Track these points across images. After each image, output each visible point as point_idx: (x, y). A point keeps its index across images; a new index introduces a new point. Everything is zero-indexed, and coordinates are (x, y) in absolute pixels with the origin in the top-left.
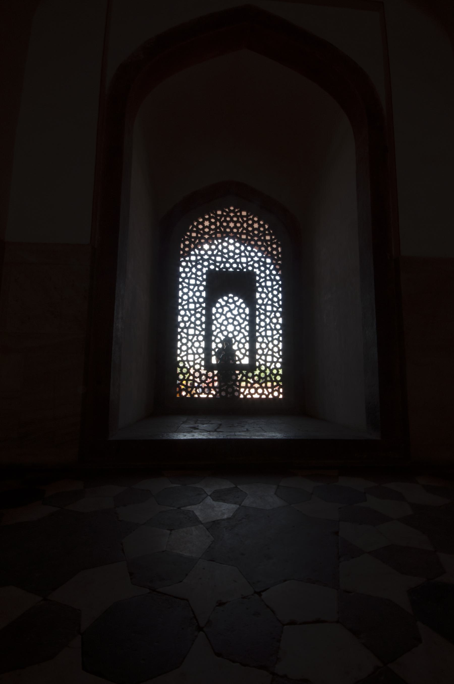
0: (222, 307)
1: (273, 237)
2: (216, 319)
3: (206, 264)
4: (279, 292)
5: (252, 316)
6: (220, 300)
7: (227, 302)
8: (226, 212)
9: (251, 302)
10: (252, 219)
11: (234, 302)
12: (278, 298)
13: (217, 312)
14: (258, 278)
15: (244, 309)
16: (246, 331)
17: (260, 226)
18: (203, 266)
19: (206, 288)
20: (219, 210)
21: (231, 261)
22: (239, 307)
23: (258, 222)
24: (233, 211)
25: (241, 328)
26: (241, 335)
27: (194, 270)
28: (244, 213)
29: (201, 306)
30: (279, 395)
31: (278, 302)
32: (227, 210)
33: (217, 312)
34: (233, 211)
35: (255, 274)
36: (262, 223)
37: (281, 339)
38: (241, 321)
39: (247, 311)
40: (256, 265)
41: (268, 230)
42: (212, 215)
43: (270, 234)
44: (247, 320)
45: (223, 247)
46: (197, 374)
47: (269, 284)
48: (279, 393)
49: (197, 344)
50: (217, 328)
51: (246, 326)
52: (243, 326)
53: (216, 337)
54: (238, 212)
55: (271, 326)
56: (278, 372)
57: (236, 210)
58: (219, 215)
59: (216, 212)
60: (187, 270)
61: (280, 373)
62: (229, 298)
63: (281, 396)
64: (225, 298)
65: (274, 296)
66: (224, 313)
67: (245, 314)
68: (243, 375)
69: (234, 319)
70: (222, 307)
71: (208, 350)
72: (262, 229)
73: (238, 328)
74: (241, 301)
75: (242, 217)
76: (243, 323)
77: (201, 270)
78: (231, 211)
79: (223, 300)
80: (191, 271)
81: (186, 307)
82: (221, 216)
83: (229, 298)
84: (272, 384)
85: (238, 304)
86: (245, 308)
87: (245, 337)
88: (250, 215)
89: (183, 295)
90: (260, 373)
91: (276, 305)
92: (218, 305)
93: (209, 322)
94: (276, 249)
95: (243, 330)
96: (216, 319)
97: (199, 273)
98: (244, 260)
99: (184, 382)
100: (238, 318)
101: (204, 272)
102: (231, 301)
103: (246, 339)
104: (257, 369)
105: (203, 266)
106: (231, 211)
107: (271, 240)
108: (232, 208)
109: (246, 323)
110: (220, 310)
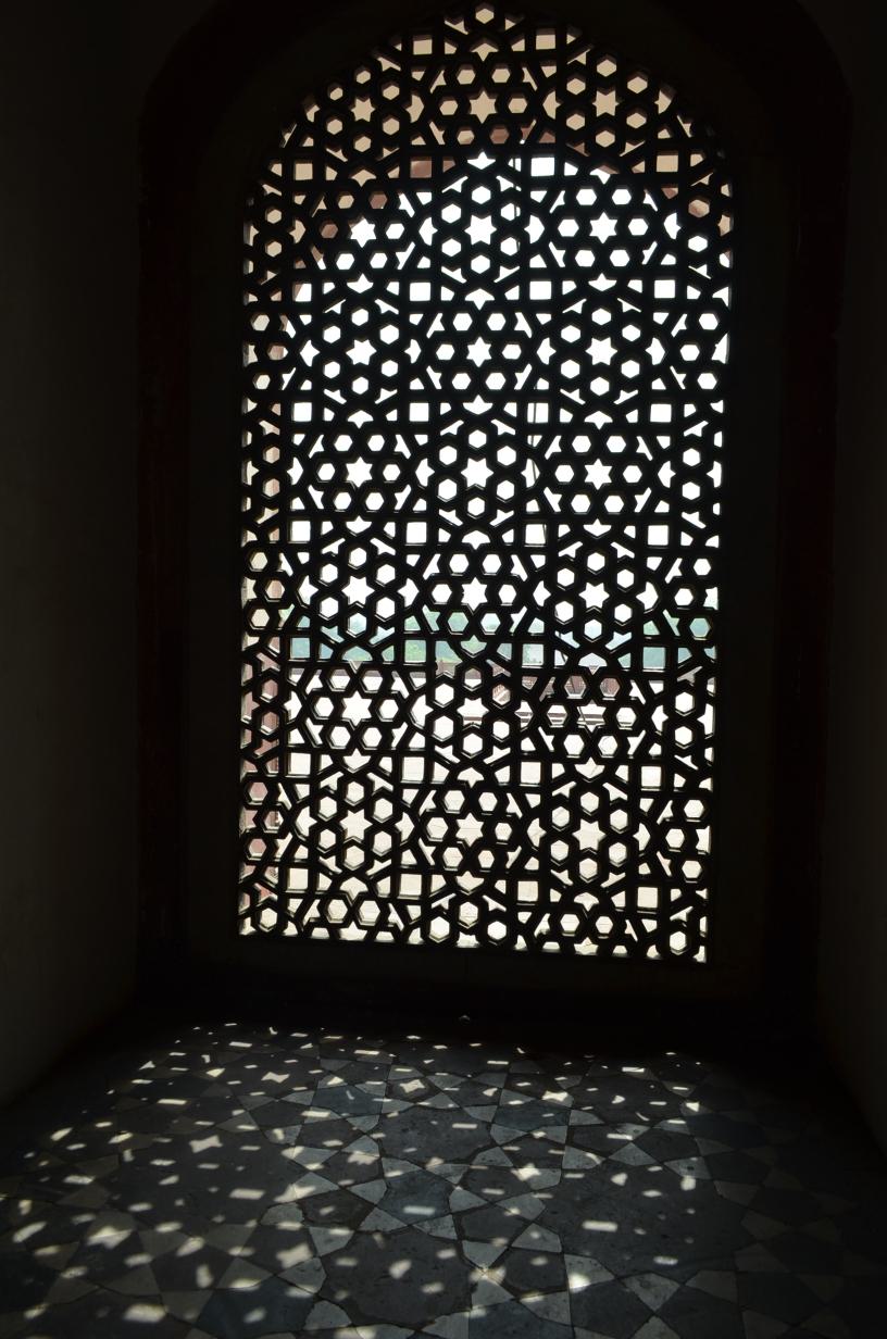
1: (696, 159)
4: (709, 454)
8: (455, 37)
12: (706, 483)
17: (628, 103)
20: (422, 35)
23: (617, 83)
24: (492, 32)
28: (546, 42)
32: (460, 27)
34: (492, 32)
36: (637, 85)
41: (668, 119)
42: (386, 64)
43: (680, 146)
47: (661, 413)
56: (691, 839)
58: (421, 61)
59: (408, 47)
65: (684, 474)
75: (535, 59)
78: (479, 32)
82: (432, 63)
88: (576, 48)
91: (693, 518)
106: (479, 32)
108: (485, 16)
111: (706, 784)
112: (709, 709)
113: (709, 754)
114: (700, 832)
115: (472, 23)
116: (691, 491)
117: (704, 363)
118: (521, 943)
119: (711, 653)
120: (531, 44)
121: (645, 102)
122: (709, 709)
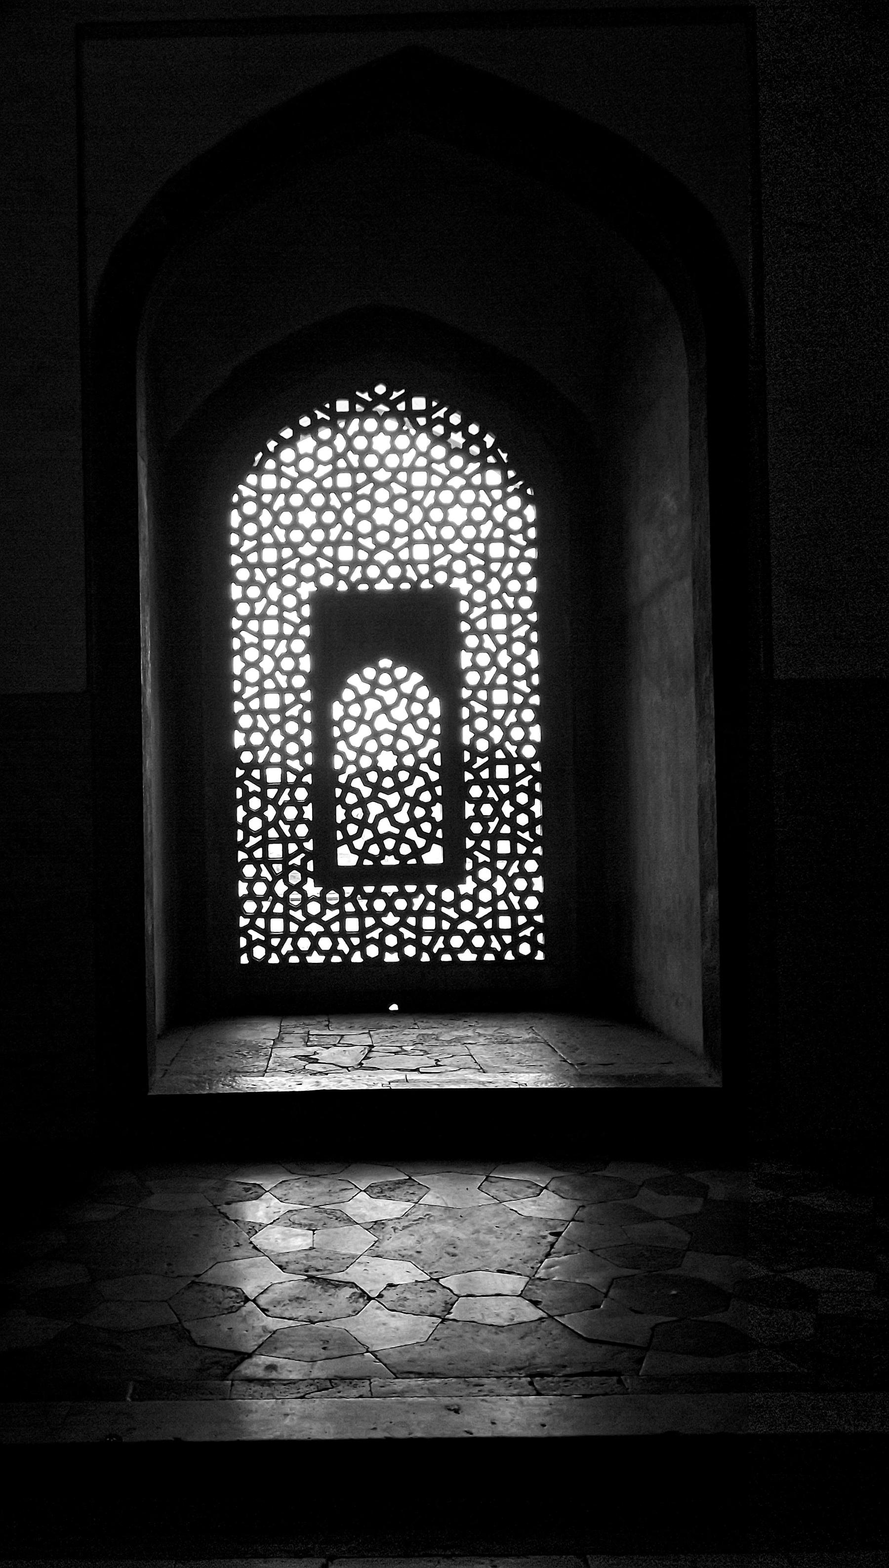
0: (360, 699)
1: (511, 474)
2: (345, 736)
3: (308, 570)
5: (451, 722)
6: (354, 680)
7: (374, 684)
8: (362, 402)
9: (445, 680)
10: (445, 421)
11: (396, 684)
13: (347, 716)
14: (464, 607)
15: (425, 703)
16: (433, 767)
17: (470, 440)
18: (301, 579)
19: (312, 646)
20: (343, 397)
21: (384, 557)
22: (412, 698)
23: (462, 428)
24: (383, 399)
26: (419, 782)
27: (274, 592)
28: (419, 403)
30: (533, 953)
31: (527, 677)
32: (366, 396)
34: (383, 399)
35: (454, 597)
38: (418, 739)
39: (435, 708)
40: (459, 567)
41: (493, 451)
42: (320, 415)
43: (500, 465)
45: (359, 517)
48: (535, 946)
49: (291, 813)
50: (347, 763)
51: (432, 753)
52: (423, 753)
54: (399, 400)
57: (395, 395)
58: (343, 415)
59: (333, 406)
60: (254, 592)
63: (540, 956)
64: (369, 672)
66: (368, 717)
68: (428, 898)
69: (397, 735)
70: (360, 699)
72: (475, 450)
73: (409, 760)
74: (417, 677)
76: (423, 745)
77: (292, 591)
78: (378, 399)
79: (364, 679)
83: (380, 671)
85: (407, 688)
86: (429, 699)
87: (429, 786)
89: (244, 670)
90: (476, 891)
91: (522, 685)
92: (348, 695)
94: (519, 513)
95: (424, 767)
96: (345, 736)
97: (290, 601)
98: (421, 552)
99: (260, 923)
101: (305, 596)
102: (385, 679)
103: (433, 793)
104: (469, 879)
105: (301, 579)
106: (378, 399)
108: (380, 389)
109: (433, 744)
110: (355, 710)
111: (538, 850)
112: (538, 802)
113: (539, 830)
114: (534, 880)
115: (372, 394)
117: (523, 592)
118: (425, 958)
119: (537, 767)
120: (409, 405)
121: (478, 440)
122: (538, 802)
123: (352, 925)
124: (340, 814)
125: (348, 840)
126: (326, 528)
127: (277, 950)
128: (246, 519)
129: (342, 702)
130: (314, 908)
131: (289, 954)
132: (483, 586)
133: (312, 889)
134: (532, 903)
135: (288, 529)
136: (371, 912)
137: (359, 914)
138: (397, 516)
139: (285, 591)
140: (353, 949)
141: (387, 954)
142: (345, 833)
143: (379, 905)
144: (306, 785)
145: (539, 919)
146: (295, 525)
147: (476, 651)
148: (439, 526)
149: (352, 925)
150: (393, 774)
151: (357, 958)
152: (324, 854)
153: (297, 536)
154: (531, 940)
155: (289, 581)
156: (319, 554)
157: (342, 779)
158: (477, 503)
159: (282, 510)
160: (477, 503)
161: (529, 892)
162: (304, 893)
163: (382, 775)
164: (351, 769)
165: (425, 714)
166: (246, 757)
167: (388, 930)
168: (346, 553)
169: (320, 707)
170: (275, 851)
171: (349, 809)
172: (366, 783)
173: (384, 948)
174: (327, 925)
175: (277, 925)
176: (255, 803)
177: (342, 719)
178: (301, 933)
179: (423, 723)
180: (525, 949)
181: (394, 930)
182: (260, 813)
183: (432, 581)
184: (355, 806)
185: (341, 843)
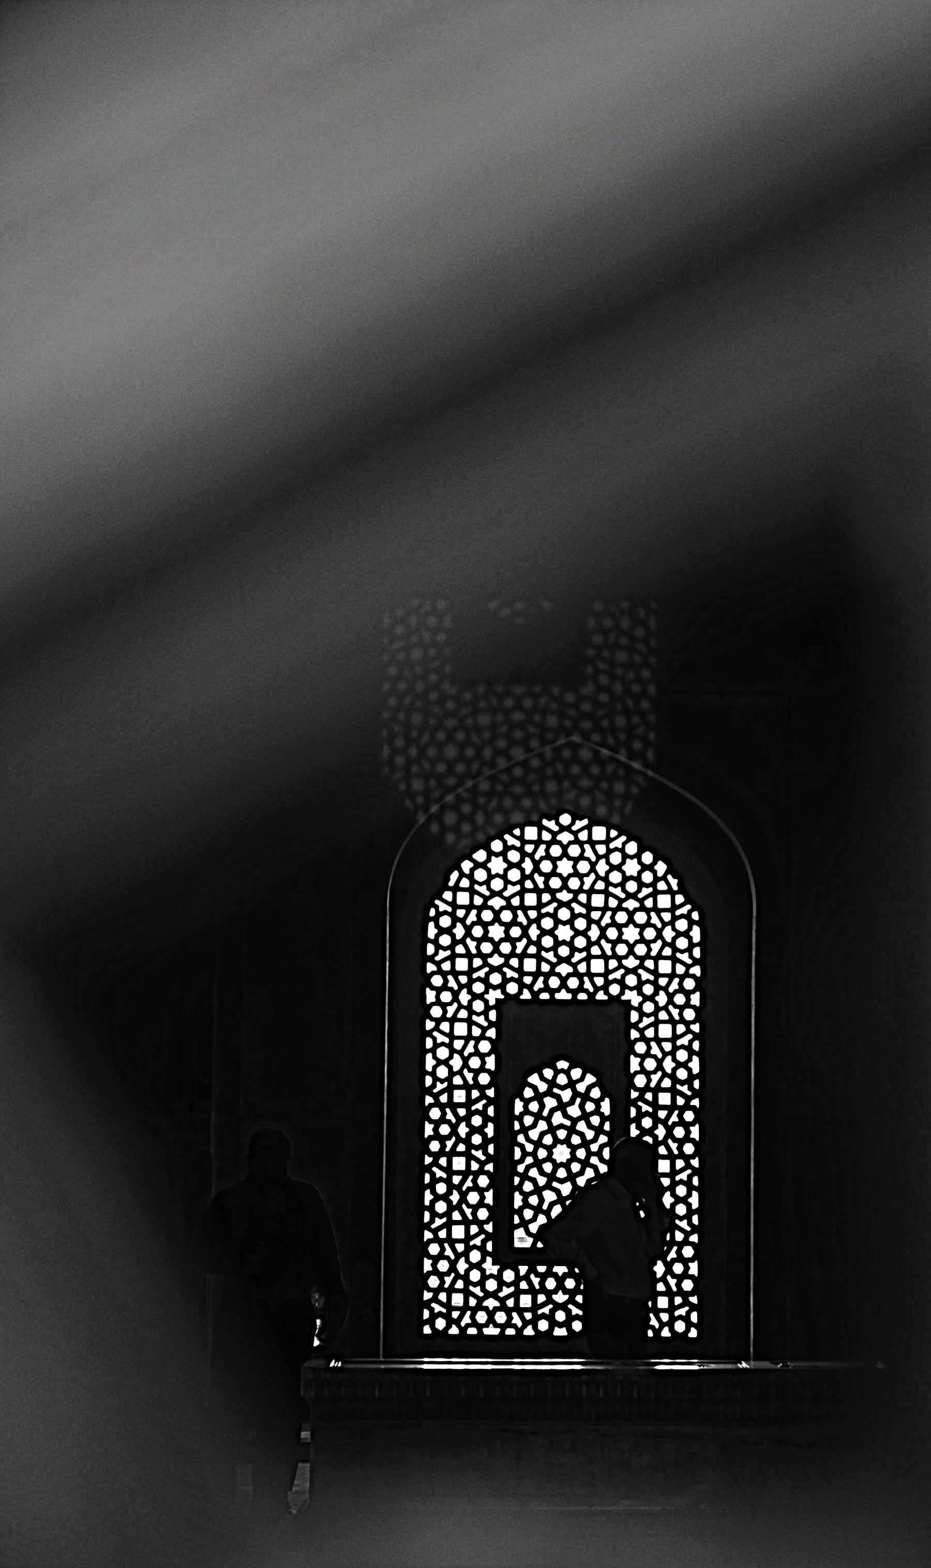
0: (539, 1097)
3: (496, 979)
5: (620, 1119)
6: (534, 1079)
7: (552, 1083)
9: (616, 1083)
13: (527, 1111)
14: (634, 1017)
15: (597, 1102)
16: (602, 1160)
22: (586, 1097)
24: (568, 829)
25: (589, 1154)
29: (483, 1096)
30: (688, 1330)
33: (527, 1111)
34: (568, 829)
37: (696, 1181)
39: (606, 1107)
41: (664, 878)
43: (670, 891)
44: (605, 1133)
46: (475, 1276)
47: (665, 1031)
48: (689, 1325)
49: (473, 1198)
50: (525, 1154)
51: (602, 1147)
53: (525, 1177)
55: (668, 1148)
60: (446, 997)
61: (690, 1272)
62: (557, 1072)
63: (693, 1333)
64: (548, 1073)
67: (601, 1115)
69: (572, 1130)
70: (539, 1097)
71: (503, 1214)
74: (590, 1079)
76: (595, 1140)
77: (481, 997)
78: (563, 829)
79: (542, 1078)
80: (456, 998)
81: (444, 1098)
83: (557, 1072)
84: (671, 1302)
86: (602, 1099)
92: (528, 1093)
93: (505, 1138)
94: (686, 934)
95: (594, 1160)
96: (525, 1130)
98: (597, 966)
100: (581, 1126)
101: (492, 1003)
102: (562, 1079)
105: (489, 986)
106: (563, 829)
107: (674, 907)
109: (603, 1139)
116: (682, 1074)
121: (651, 868)
123: (526, 1301)
124: (518, 1200)
125: (524, 1224)
126: (513, 942)
127: (457, 1322)
128: (441, 931)
129: (522, 1099)
130: (491, 1285)
131: (468, 1326)
132: (652, 998)
133: (491, 1268)
134: (688, 1285)
135: (479, 941)
136: (543, 1290)
137: (532, 1291)
138: (577, 933)
139: (475, 997)
140: (526, 1323)
141: (556, 1328)
142: (521, 1217)
143: (551, 1284)
144: (692, 1244)
145: (694, 1300)
146: (485, 938)
147: (643, 1057)
148: (614, 943)
149: (526, 1301)
150: (567, 1165)
151: (529, 1331)
152: (502, 1236)
153: (487, 948)
154: (686, 1319)
155: (478, 988)
156: (507, 964)
157: (521, 1168)
158: (648, 924)
159: (474, 924)
160: (648, 924)
161: (685, 1275)
162: (483, 1271)
163: (556, 1166)
164: (529, 1160)
165: (597, 1112)
166: (435, 1146)
167: (557, 1306)
168: (530, 965)
169: (503, 1103)
170: (458, 1232)
171: (526, 1196)
172: (542, 1172)
173: (553, 1323)
174: (503, 1301)
175: (458, 1299)
176: (441, 1188)
177: (522, 1115)
178: (479, 1307)
179: (595, 1120)
180: (680, 1326)
181: (563, 1307)
182: (445, 1198)
183: (607, 993)
184: (531, 1193)
185: (518, 1226)
